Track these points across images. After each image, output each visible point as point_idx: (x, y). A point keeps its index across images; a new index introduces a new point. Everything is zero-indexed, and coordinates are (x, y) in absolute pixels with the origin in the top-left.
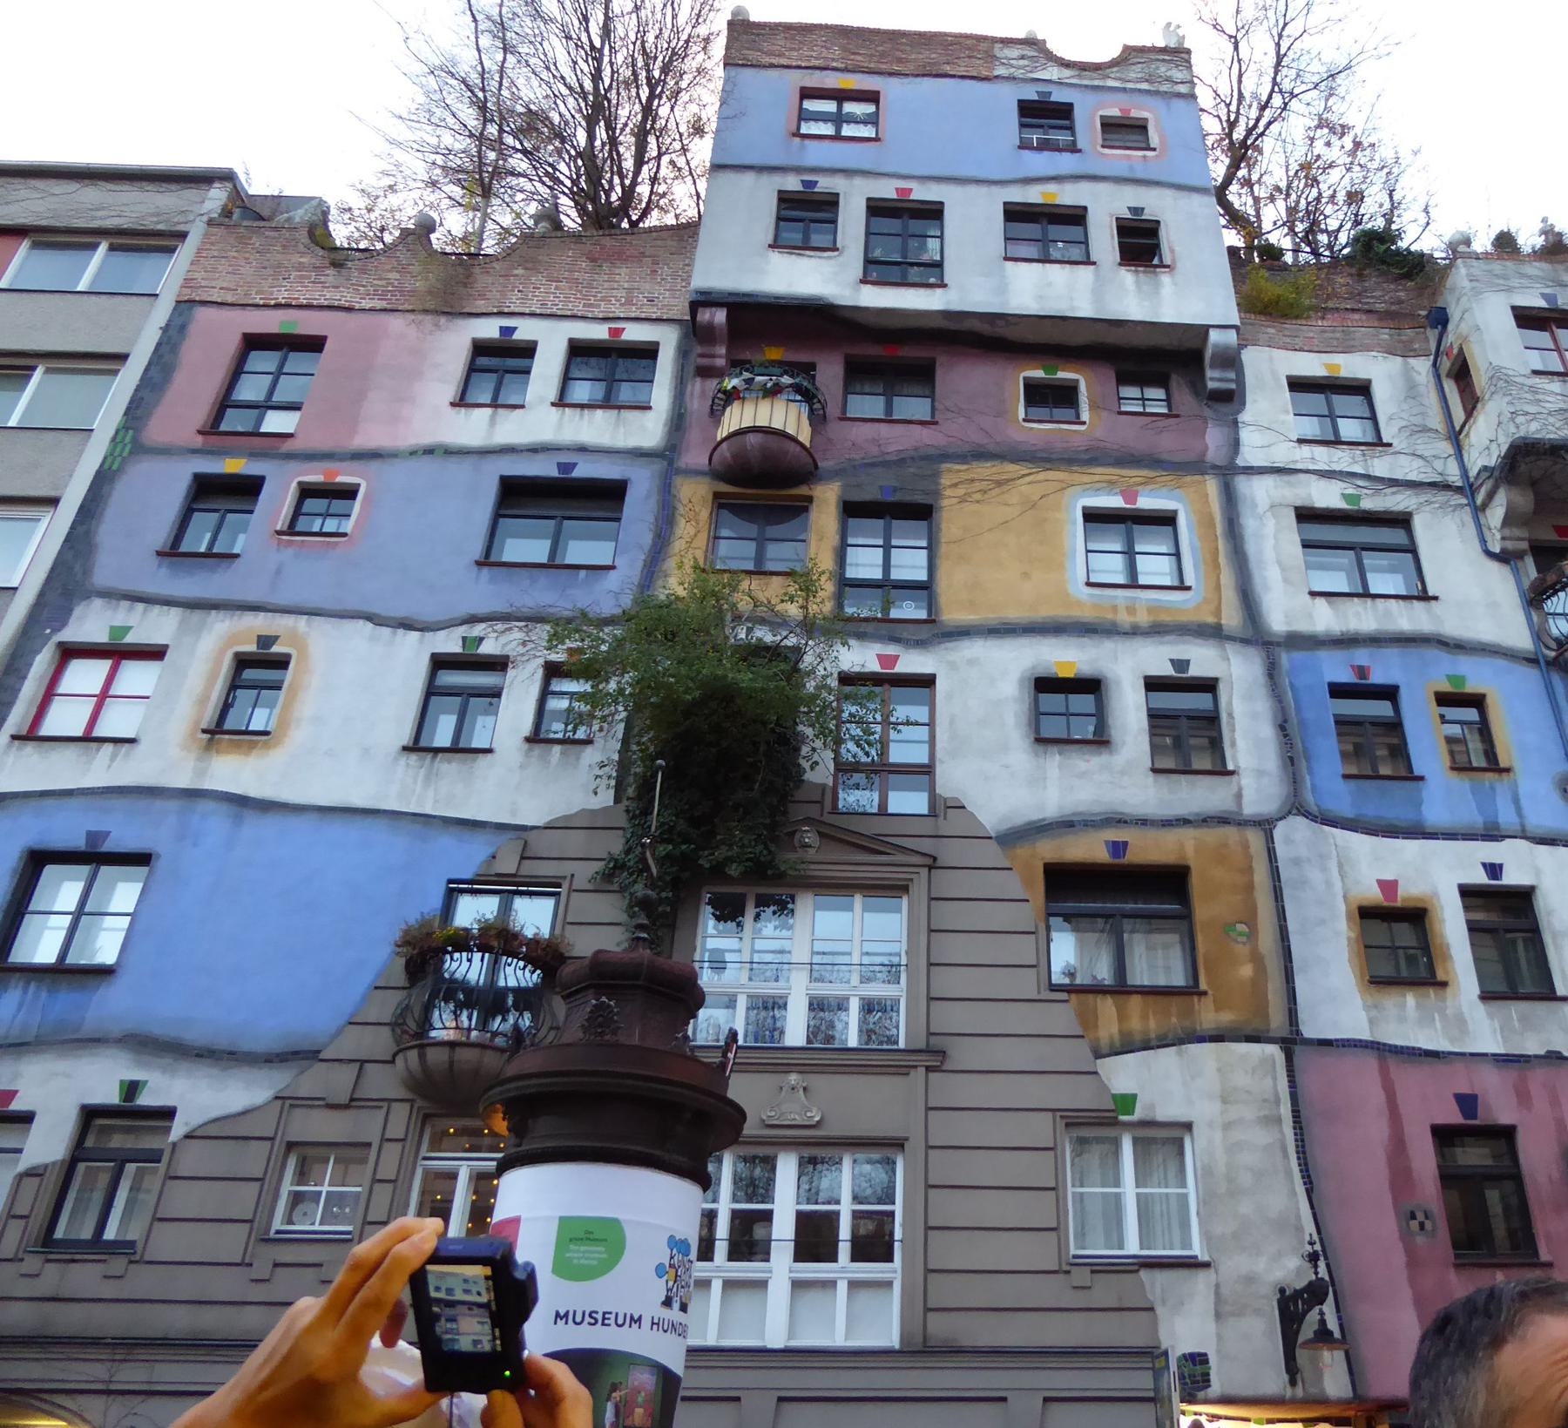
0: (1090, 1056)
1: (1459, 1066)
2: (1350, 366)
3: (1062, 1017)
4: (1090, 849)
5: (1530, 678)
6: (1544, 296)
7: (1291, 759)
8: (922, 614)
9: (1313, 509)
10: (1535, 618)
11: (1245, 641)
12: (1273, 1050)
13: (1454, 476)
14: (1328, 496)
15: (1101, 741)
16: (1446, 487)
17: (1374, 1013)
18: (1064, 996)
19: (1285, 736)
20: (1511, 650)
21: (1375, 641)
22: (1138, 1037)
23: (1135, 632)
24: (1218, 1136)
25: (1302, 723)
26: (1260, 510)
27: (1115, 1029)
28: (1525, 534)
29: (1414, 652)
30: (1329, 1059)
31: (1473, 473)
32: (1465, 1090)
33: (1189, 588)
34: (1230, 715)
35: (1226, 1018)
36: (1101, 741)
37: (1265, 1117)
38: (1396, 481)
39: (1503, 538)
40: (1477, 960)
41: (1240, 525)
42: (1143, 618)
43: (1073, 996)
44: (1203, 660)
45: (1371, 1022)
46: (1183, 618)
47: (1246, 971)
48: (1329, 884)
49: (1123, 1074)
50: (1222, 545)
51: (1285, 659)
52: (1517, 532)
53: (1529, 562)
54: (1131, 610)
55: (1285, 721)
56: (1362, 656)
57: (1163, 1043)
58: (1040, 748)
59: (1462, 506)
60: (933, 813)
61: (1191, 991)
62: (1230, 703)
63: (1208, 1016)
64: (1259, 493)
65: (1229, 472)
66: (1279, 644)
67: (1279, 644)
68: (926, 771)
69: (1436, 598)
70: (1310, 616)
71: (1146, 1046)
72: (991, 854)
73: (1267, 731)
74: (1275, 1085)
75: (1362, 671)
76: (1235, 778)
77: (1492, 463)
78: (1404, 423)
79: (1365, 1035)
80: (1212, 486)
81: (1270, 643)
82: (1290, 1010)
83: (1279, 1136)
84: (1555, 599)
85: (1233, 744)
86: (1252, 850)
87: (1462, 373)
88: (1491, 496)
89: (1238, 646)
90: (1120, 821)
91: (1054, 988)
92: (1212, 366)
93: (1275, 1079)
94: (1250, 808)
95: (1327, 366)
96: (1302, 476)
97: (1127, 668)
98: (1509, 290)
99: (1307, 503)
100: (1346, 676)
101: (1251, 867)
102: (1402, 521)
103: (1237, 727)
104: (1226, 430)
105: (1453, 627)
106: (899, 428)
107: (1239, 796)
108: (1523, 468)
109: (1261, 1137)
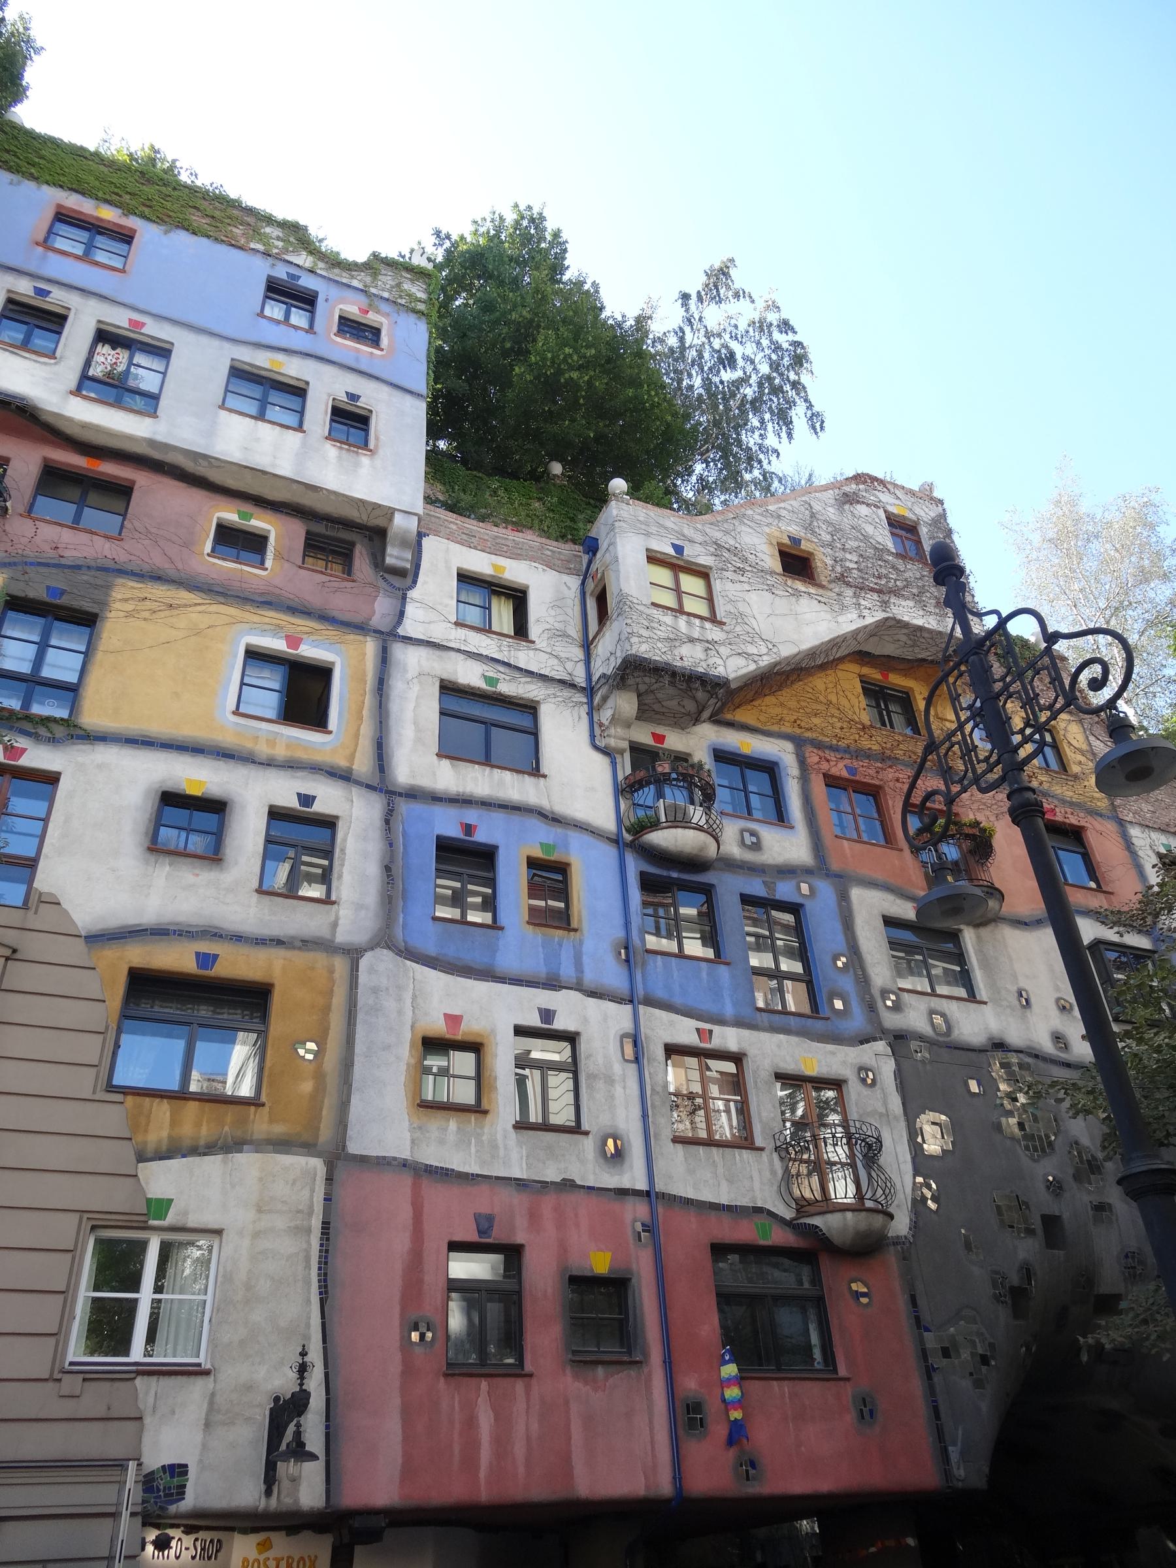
0: (133, 1158)
1: (485, 1187)
2: (515, 571)
3: (111, 1117)
4: (177, 958)
5: (609, 853)
6: (675, 546)
7: (390, 897)
8: (63, 713)
9: (454, 683)
11: (368, 786)
12: (317, 1164)
13: (580, 679)
14: (470, 675)
15: (214, 856)
16: (573, 686)
17: (418, 1134)
18: (118, 1097)
19: (388, 876)
20: (597, 828)
21: (486, 804)
22: (187, 1143)
23: (269, 763)
24: (246, 1242)
26: (409, 676)
27: (165, 1134)
29: (516, 818)
31: (595, 678)
32: (484, 1209)
33: (331, 732)
34: (343, 851)
35: (279, 1129)
36: (214, 856)
37: (297, 1227)
38: (531, 673)
41: (389, 686)
42: (280, 752)
43: (130, 1100)
44: (329, 798)
45: (413, 1141)
46: (319, 758)
47: (307, 1087)
48: (400, 1012)
49: (161, 1179)
50: (369, 700)
52: (620, 731)
53: (627, 756)
54: (272, 743)
55: (392, 861)
56: (471, 816)
57: (209, 1149)
58: (152, 858)
59: (582, 703)
60: (25, 906)
61: (253, 1102)
62: (345, 840)
63: (260, 1125)
64: (410, 660)
65: (389, 638)
66: (400, 795)
67: (400, 795)
68: (31, 864)
69: (545, 776)
70: (434, 774)
71: (194, 1151)
72: (76, 951)
73: (373, 870)
74: (312, 1197)
75: (469, 829)
77: (609, 673)
78: (548, 627)
79: (405, 1154)
80: (370, 647)
81: (394, 793)
83: (304, 1246)
84: (641, 792)
85: (340, 877)
86: (337, 975)
87: (602, 599)
88: (605, 699)
89: (364, 791)
90: (214, 934)
91: (111, 1088)
92: (393, 546)
93: (312, 1191)
94: (343, 936)
95: (495, 566)
96: (453, 654)
97: (254, 796)
98: (648, 534)
99: (452, 678)
100: (453, 831)
101: (332, 991)
102: (530, 709)
103: (346, 863)
104: (394, 601)
106: (84, 537)
107: (335, 925)
108: (631, 681)
109: (288, 1246)
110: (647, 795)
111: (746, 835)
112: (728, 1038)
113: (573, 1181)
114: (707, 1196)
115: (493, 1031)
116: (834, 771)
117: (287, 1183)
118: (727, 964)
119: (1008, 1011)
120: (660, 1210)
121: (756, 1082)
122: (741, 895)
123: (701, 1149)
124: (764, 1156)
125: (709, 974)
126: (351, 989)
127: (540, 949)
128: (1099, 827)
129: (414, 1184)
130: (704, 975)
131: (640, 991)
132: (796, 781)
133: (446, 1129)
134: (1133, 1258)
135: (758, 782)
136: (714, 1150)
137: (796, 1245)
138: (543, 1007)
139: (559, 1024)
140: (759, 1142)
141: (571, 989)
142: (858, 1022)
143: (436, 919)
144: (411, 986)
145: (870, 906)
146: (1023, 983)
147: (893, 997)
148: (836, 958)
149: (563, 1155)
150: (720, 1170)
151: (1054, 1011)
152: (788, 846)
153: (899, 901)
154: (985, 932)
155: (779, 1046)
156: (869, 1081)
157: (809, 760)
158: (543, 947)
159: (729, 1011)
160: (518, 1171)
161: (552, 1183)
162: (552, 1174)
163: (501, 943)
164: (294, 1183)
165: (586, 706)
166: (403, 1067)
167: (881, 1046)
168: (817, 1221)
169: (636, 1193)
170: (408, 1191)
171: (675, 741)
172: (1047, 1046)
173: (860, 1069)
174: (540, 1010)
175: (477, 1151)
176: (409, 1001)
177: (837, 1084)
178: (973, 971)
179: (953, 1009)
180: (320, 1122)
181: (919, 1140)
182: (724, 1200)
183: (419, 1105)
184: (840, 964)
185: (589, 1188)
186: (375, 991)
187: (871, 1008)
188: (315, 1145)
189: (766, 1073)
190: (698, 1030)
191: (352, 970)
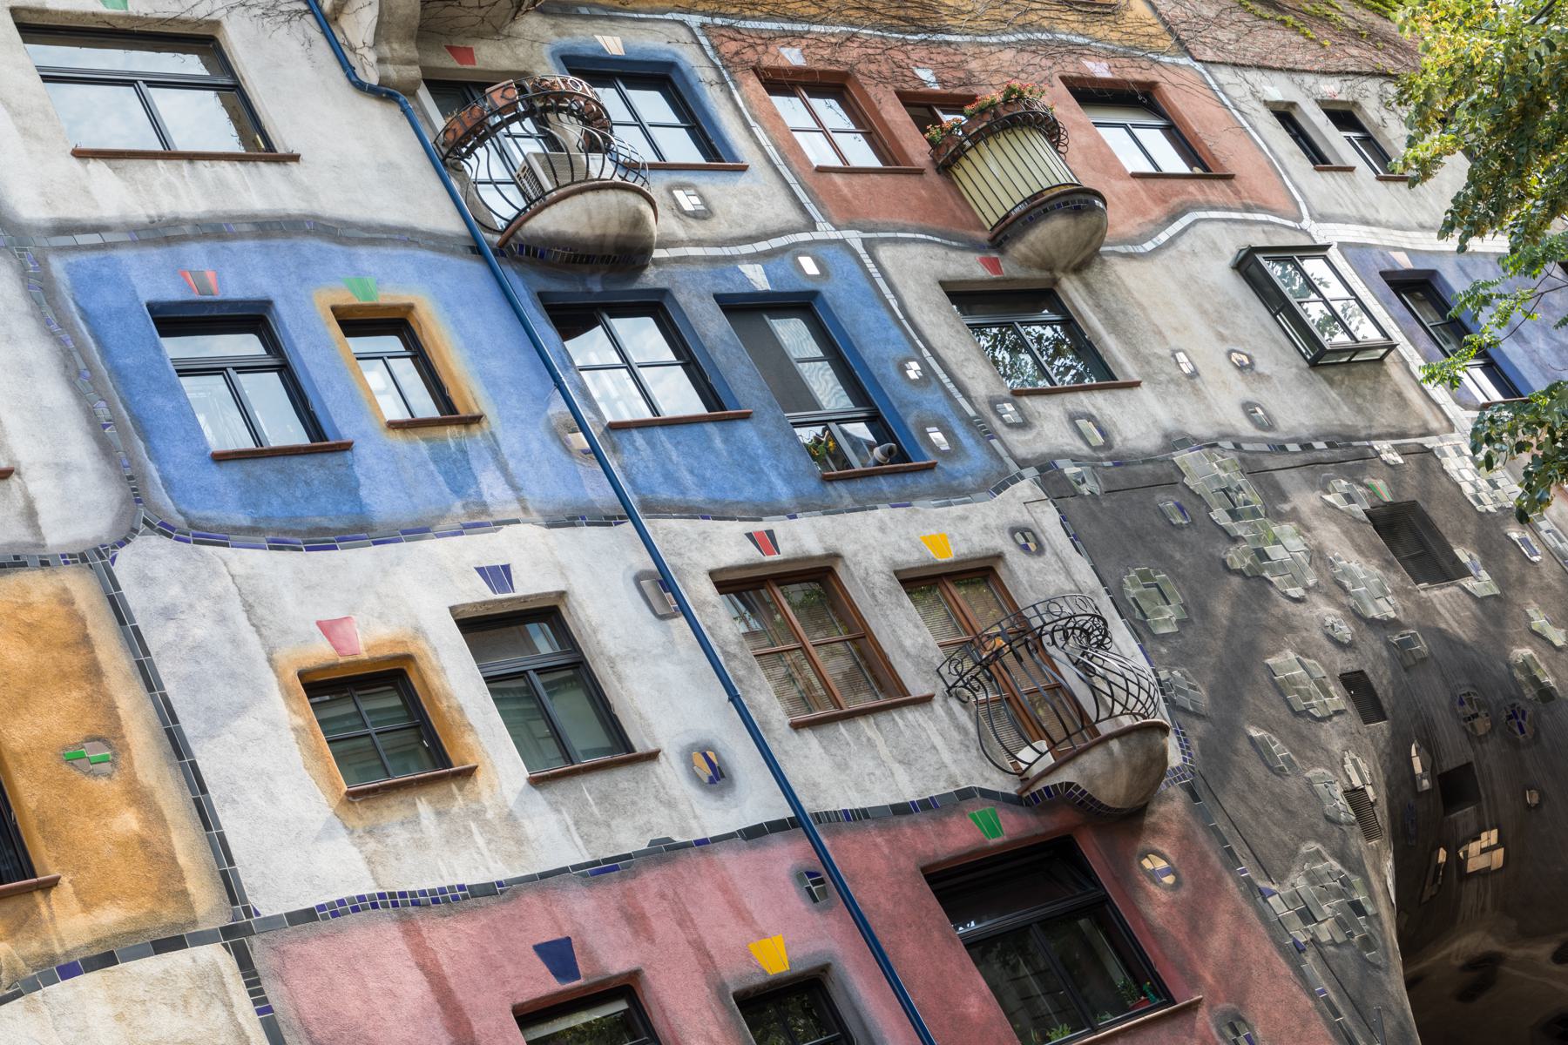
9: (43, 12)
10: (456, 185)
12: (216, 955)
17: (372, 845)
21: (213, 230)
25: (117, 372)
28: (415, 54)
30: (313, 947)
35: (110, 917)
39: (381, 61)
40: (503, 714)
45: (369, 861)
48: (235, 642)
51: (57, 266)
53: (424, 94)
56: (196, 255)
63: (70, 922)
69: (295, 158)
70: (86, 191)
74: (232, 1014)
76: (14, 477)
79: (368, 888)
82: (224, 875)
93: (229, 1006)
94: (57, 537)
100: (172, 292)
105: (333, 204)
107: (30, 514)
110: (483, 164)
111: (679, 194)
112: (803, 537)
113: (669, 840)
114: (881, 797)
115: (418, 631)
116: (767, 61)
117: (174, 1006)
118: (746, 417)
119: (1172, 388)
120: (825, 842)
121: (873, 596)
122: (719, 298)
123: (841, 728)
124: (937, 705)
125: (726, 441)
126: (122, 622)
127: (432, 467)
128: (1174, 79)
129: (406, 933)
130: (718, 443)
131: (633, 499)
132: (717, 88)
133: (416, 820)
134: (1471, 704)
135: (652, 104)
136: (861, 723)
137: (1041, 830)
138: (484, 564)
139: (529, 584)
140: (917, 687)
141: (517, 522)
142: (975, 459)
143: (221, 458)
144: (233, 589)
145: (916, 270)
146: (1174, 344)
147: (1009, 407)
148: (902, 370)
149: (633, 803)
150: (884, 750)
151: (1233, 375)
152: (751, 201)
153: (953, 255)
154: (1092, 275)
155: (882, 529)
156: (1032, 546)
157: (723, 50)
158: (435, 462)
159: (784, 492)
160: (573, 853)
161: (638, 854)
162: (629, 839)
163: (358, 471)
164: (186, 1003)
165: (310, 18)
166: (292, 735)
167: (1026, 488)
168: (1068, 775)
169: (777, 826)
170: (401, 945)
171: (489, 56)
172: (1246, 428)
173: (1013, 531)
174: (480, 570)
175: (489, 842)
176: (242, 618)
177: (981, 572)
178: (1100, 339)
179: (1099, 403)
180: (182, 879)
181: (1138, 615)
182: (909, 794)
183: (353, 795)
184: (912, 375)
185: (699, 843)
186: (168, 613)
187: (990, 434)
188: (194, 923)
189: (882, 581)
190: (749, 535)
191: (106, 590)
